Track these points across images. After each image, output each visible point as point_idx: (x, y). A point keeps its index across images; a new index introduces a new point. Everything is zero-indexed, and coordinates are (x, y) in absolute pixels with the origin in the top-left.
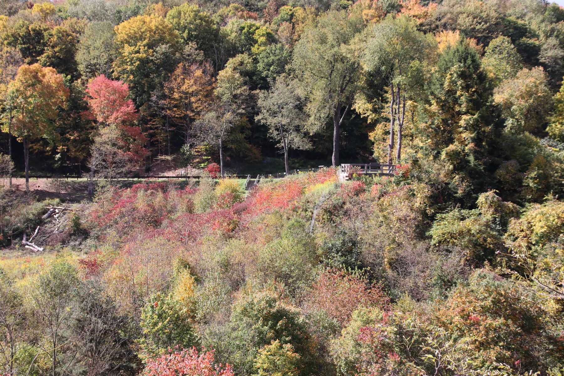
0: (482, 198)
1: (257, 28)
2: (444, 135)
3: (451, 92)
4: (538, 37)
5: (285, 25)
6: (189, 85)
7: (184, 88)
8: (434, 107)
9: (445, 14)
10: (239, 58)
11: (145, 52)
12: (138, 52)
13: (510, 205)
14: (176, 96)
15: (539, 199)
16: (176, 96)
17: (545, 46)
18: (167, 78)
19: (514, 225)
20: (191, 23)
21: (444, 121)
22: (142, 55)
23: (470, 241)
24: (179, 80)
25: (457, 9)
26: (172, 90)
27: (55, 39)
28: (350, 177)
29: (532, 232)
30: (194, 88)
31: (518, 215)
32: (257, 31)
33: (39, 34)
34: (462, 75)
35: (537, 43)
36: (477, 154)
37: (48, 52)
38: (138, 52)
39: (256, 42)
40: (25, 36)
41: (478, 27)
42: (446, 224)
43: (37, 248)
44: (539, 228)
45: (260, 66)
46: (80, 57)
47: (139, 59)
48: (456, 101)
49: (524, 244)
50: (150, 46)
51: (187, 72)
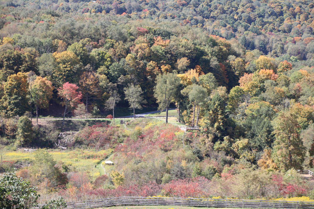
0: (225, 138)
1: (105, 54)
2: (213, 121)
3: (216, 109)
4: (207, 55)
5: (112, 49)
6: (89, 82)
7: (87, 82)
8: (211, 112)
9: (174, 46)
10: (102, 68)
11: (70, 67)
12: (66, 67)
13: (232, 140)
14: (84, 85)
15: (238, 137)
16: (84, 85)
17: (212, 60)
18: (80, 79)
19: (234, 145)
20: (81, 53)
21: (214, 117)
22: (69, 69)
23: (225, 149)
24: (84, 79)
25: (177, 42)
26: (82, 83)
27: (27, 59)
28: (187, 130)
29: (239, 147)
30: (91, 83)
31: (234, 142)
32: (105, 55)
33: (19, 57)
34: (219, 105)
35: (208, 58)
36: (223, 126)
37: (25, 65)
38: (66, 67)
39: (106, 60)
40: (13, 58)
41: (186, 51)
42: (217, 145)
43: (63, 148)
44: (241, 146)
45: (111, 71)
46: (41, 68)
47: (67, 70)
48: (217, 111)
49: (237, 150)
50: (71, 64)
51: (87, 77)
